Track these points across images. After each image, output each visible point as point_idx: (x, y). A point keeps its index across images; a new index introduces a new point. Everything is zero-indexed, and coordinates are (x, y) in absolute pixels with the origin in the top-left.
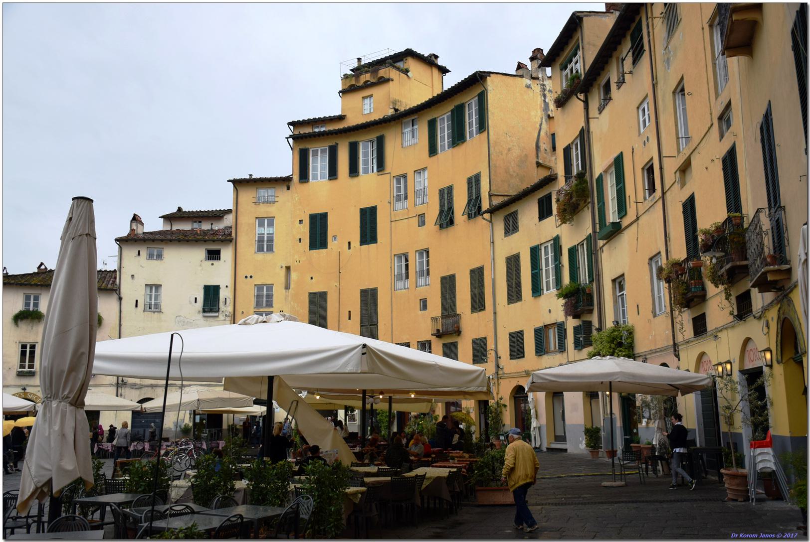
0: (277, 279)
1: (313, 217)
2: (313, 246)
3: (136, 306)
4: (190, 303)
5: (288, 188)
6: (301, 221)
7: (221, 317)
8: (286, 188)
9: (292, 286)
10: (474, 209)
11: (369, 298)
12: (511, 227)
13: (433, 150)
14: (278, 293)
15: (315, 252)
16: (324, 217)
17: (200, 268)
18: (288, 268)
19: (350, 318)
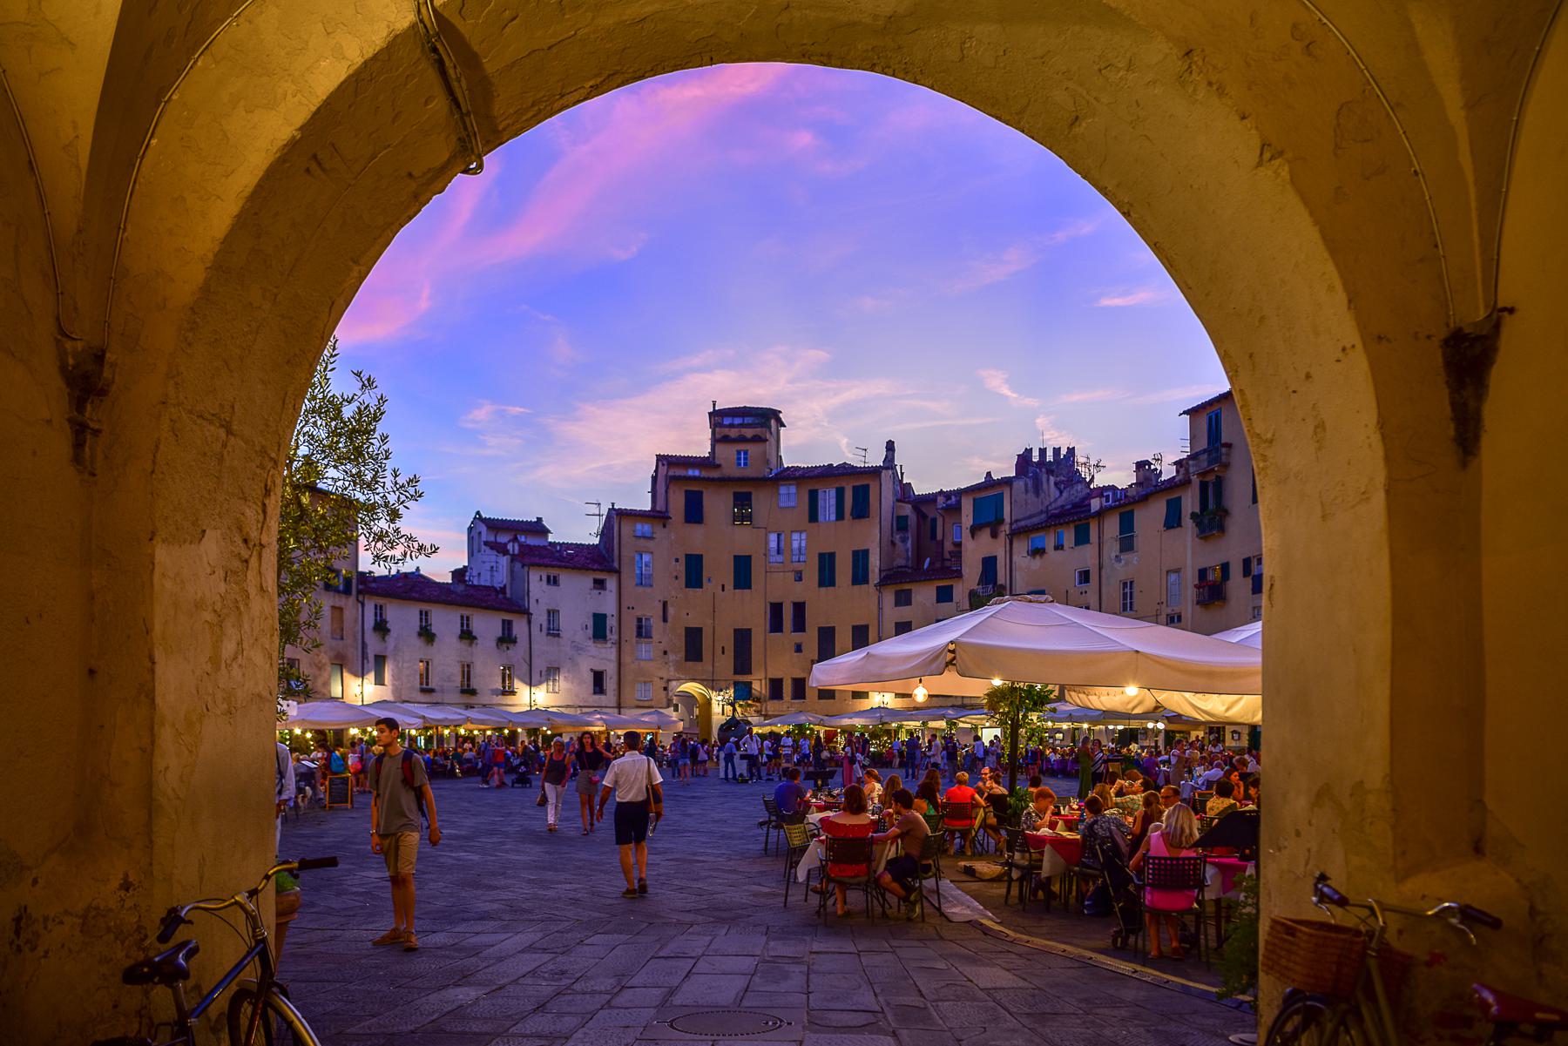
0: (652, 612)
1: (689, 557)
2: (688, 585)
3: (541, 630)
4: (582, 629)
5: (664, 526)
6: (677, 560)
7: (609, 645)
8: (662, 526)
9: (670, 619)
10: (860, 577)
11: (743, 639)
12: (903, 599)
13: (813, 517)
14: (656, 625)
15: (691, 591)
16: (699, 558)
17: (589, 596)
18: (665, 604)
19: (723, 653)
